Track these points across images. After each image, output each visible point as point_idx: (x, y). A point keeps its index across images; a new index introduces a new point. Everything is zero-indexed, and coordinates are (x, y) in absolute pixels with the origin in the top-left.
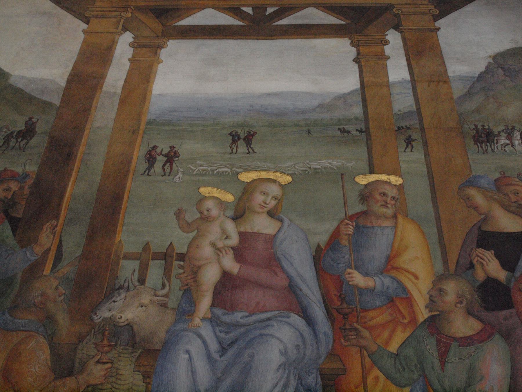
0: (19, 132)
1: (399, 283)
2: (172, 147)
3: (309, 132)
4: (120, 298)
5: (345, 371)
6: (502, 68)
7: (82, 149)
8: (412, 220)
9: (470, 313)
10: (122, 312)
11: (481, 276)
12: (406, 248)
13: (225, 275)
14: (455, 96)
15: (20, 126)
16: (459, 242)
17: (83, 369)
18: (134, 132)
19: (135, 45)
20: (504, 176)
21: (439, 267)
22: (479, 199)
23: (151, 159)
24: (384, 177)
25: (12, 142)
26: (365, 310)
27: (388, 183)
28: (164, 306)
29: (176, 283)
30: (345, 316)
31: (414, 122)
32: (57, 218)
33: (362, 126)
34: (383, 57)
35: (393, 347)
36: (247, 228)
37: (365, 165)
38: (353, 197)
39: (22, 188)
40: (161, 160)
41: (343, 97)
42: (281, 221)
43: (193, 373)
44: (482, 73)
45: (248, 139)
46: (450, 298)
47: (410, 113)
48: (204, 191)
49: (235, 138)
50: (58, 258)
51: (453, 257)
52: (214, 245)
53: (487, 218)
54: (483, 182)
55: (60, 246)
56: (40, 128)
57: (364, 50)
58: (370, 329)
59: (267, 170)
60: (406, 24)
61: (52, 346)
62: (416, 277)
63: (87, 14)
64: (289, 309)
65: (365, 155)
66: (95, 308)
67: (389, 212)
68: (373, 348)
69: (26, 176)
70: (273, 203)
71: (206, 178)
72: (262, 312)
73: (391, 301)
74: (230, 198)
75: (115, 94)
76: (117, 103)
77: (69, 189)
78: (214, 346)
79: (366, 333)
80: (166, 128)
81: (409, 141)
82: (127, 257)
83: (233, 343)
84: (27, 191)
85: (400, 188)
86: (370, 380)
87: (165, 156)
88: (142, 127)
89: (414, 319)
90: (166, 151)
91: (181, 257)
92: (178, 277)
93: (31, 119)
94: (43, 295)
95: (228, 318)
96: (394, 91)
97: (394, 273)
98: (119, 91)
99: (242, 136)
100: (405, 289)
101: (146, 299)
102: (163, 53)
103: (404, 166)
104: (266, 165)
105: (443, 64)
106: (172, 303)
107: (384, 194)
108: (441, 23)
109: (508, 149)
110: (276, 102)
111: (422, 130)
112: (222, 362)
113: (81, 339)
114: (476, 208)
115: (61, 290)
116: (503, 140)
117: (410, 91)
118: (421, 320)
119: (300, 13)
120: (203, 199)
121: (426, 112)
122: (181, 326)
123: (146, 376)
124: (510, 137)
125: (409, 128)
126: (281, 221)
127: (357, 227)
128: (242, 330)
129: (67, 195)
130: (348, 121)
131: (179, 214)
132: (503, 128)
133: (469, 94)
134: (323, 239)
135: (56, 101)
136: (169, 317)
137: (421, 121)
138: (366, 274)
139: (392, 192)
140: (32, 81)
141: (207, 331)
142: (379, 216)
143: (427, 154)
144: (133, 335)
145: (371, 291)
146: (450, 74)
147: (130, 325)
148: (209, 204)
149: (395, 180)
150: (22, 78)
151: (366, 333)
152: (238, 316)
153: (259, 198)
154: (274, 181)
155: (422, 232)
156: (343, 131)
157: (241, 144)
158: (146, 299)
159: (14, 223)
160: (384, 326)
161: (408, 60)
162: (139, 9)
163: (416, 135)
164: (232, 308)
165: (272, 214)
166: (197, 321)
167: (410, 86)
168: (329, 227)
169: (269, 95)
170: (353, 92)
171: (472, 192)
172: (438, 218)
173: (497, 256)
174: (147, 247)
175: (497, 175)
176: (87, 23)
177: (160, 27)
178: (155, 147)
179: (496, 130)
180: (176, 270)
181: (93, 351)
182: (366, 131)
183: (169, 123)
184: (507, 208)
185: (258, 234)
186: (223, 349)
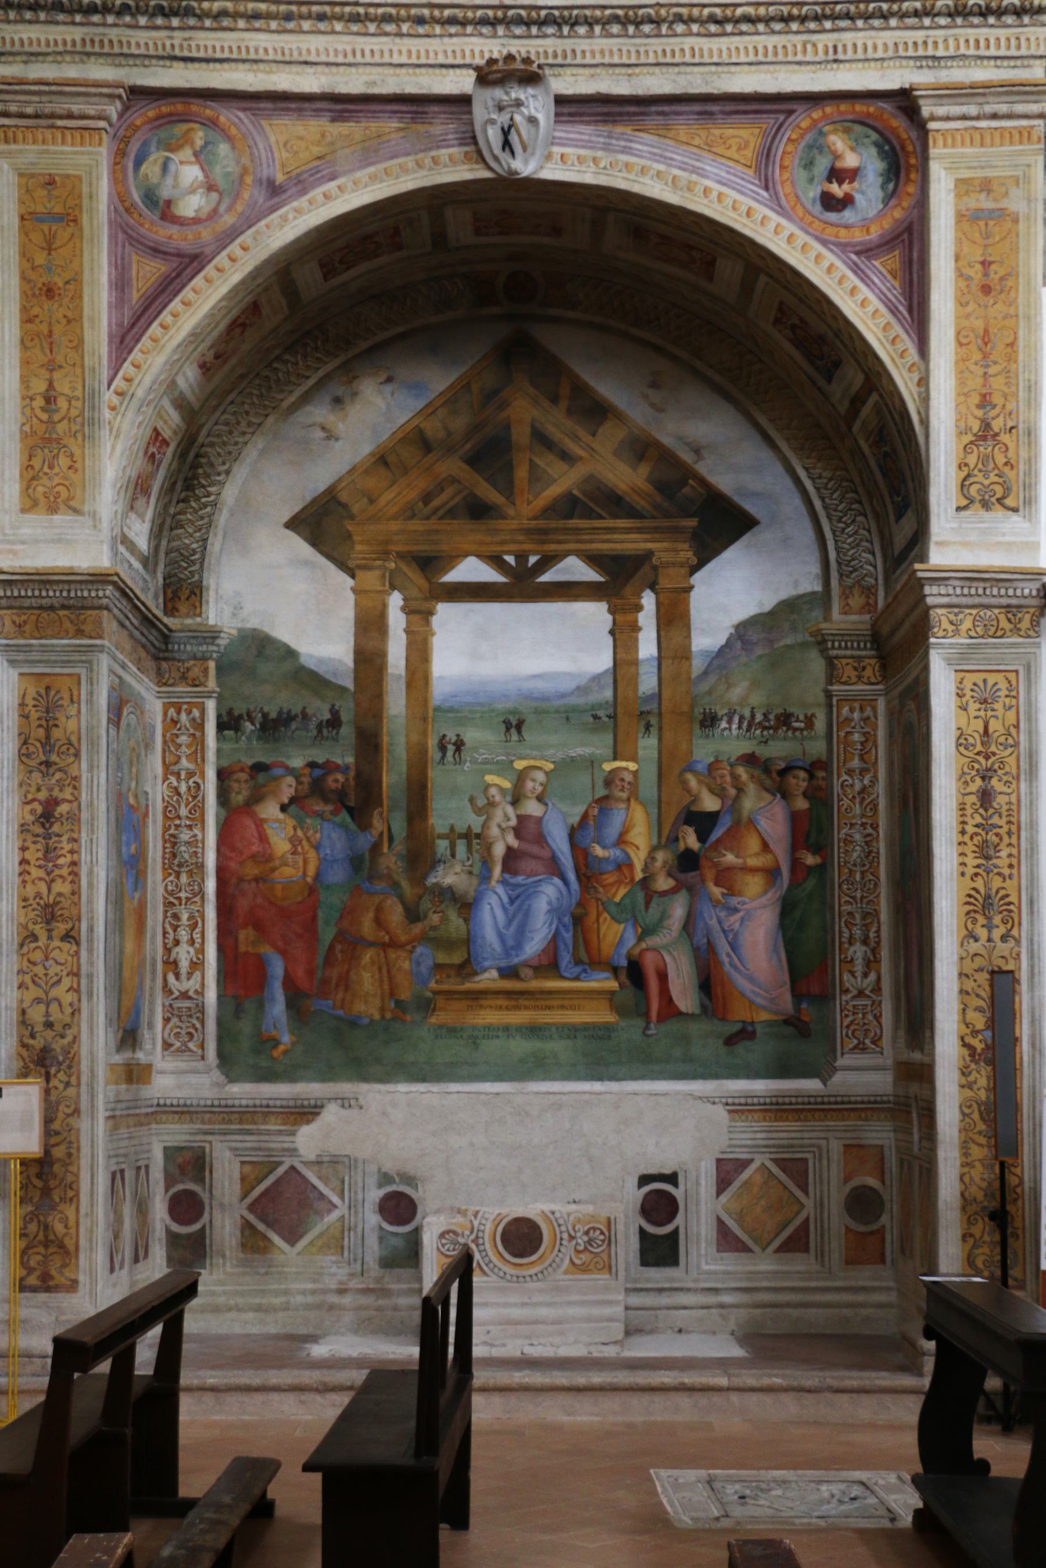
0: (328, 721)
1: (627, 854)
2: (458, 735)
3: (568, 719)
4: (441, 868)
5: (586, 914)
6: (742, 642)
7: (385, 739)
8: (641, 803)
9: (670, 875)
10: (444, 877)
11: (682, 846)
12: (634, 826)
13: (509, 849)
14: (694, 675)
15: (327, 716)
16: (672, 820)
17: (425, 917)
18: (425, 719)
19: (407, 610)
20: (717, 761)
21: (655, 841)
22: (693, 782)
23: (443, 748)
24: (623, 764)
25: (325, 732)
26: (602, 874)
27: (626, 769)
28: (470, 873)
29: (477, 856)
30: (589, 878)
31: (653, 706)
32: (381, 805)
33: (611, 711)
34: (635, 628)
35: (617, 899)
36: (522, 811)
37: (609, 752)
38: (599, 783)
39: (347, 779)
40: (451, 748)
41: (597, 678)
42: (546, 805)
43: (494, 917)
44: (723, 647)
45: (519, 727)
46: (658, 864)
47: (652, 696)
48: (490, 778)
49: (508, 725)
50: (391, 839)
51: (666, 831)
52: (499, 826)
53: (696, 799)
54: (700, 767)
55: (389, 829)
56: (345, 716)
57: (620, 618)
58: (604, 886)
59: (534, 758)
60: (664, 583)
61: (403, 903)
62: (638, 848)
63: (351, 564)
64: (553, 874)
65: (611, 743)
66: (425, 877)
67: (624, 795)
68: (605, 899)
69: (347, 767)
70: (540, 789)
71: (489, 767)
72: (536, 875)
73: (619, 867)
74: (507, 785)
75: (399, 677)
76: (404, 687)
77: (384, 779)
78: (506, 900)
79: (601, 889)
80: (450, 715)
81: (648, 727)
82: (441, 837)
83: (518, 897)
84: (352, 783)
85: (635, 773)
86: (601, 920)
87: (455, 744)
88: (431, 713)
89: (632, 879)
90: (454, 739)
91: (478, 836)
92: (477, 851)
93: (333, 706)
94: (388, 867)
95: (513, 881)
96: (642, 670)
97: (623, 846)
98: (403, 673)
99: (514, 723)
100: (629, 858)
101: (458, 868)
102: (435, 620)
103: (641, 752)
104: (534, 753)
105: (688, 636)
106: (476, 870)
107: (623, 780)
108: (697, 579)
109: (726, 733)
110: (541, 685)
111: (660, 714)
112: (511, 909)
113: (420, 897)
114: (689, 791)
115: (399, 864)
116: (724, 724)
117: (655, 670)
118: (637, 879)
119: (561, 565)
120: (488, 786)
121: (666, 695)
122: (483, 887)
123: (466, 920)
124: (730, 722)
125: (648, 713)
126: (546, 805)
127: (601, 810)
128: (523, 888)
129: (384, 785)
130: (600, 706)
131: (472, 800)
132: (726, 711)
133: (705, 673)
134: (575, 820)
135: (349, 683)
136: (475, 881)
137: (660, 704)
138: (604, 847)
139: (629, 778)
140: (321, 661)
141: (500, 890)
142: (619, 800)
143: (660, 740)
144: (453, 893)
145: (606, 860)
146: (694, 648)
147: (450, 888)
148: (493, 791)
149: (632, 766)
150: (311, 656)
151: (601, 889)
152: (520, 879)
153: (530, 785)
154: (539, 768)
155: (647, 813)
156: (596, 717)
157: (513, 731)
158: (458, 868)
159: (350, 811)
160: (612, 885)
161: (658, 632)
162: (401, 556)
163: (654, 721)
164: (515, 873)
165: (540, 799)
166: (493, 883)
167: (656, 663)
168: (579, 810)
169: (535, 677)
170: (606, 671)
171: (689, 776)
172: (660, 801)
173: (696, 831)
174: (452, 829)
175: (712, 759)
176: (353, 577)
177: (425, 585)
178: (444, 736)
179: (720, 714)
180: (475, 847)
181: (430, 905)
182: (613, 717)
183: (451, 710)
184: (712, 791)
185: (529, 817)
186: (512, 901)
